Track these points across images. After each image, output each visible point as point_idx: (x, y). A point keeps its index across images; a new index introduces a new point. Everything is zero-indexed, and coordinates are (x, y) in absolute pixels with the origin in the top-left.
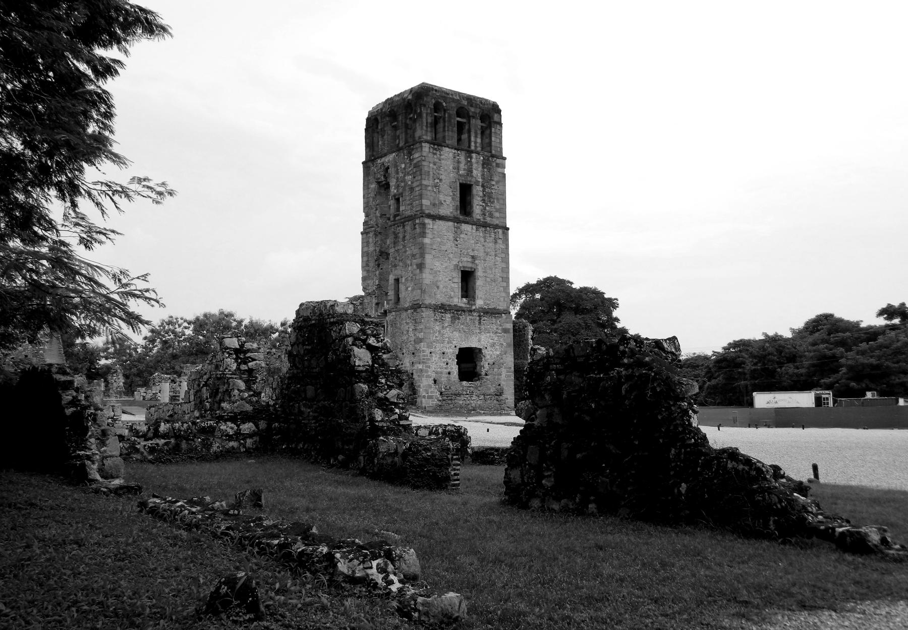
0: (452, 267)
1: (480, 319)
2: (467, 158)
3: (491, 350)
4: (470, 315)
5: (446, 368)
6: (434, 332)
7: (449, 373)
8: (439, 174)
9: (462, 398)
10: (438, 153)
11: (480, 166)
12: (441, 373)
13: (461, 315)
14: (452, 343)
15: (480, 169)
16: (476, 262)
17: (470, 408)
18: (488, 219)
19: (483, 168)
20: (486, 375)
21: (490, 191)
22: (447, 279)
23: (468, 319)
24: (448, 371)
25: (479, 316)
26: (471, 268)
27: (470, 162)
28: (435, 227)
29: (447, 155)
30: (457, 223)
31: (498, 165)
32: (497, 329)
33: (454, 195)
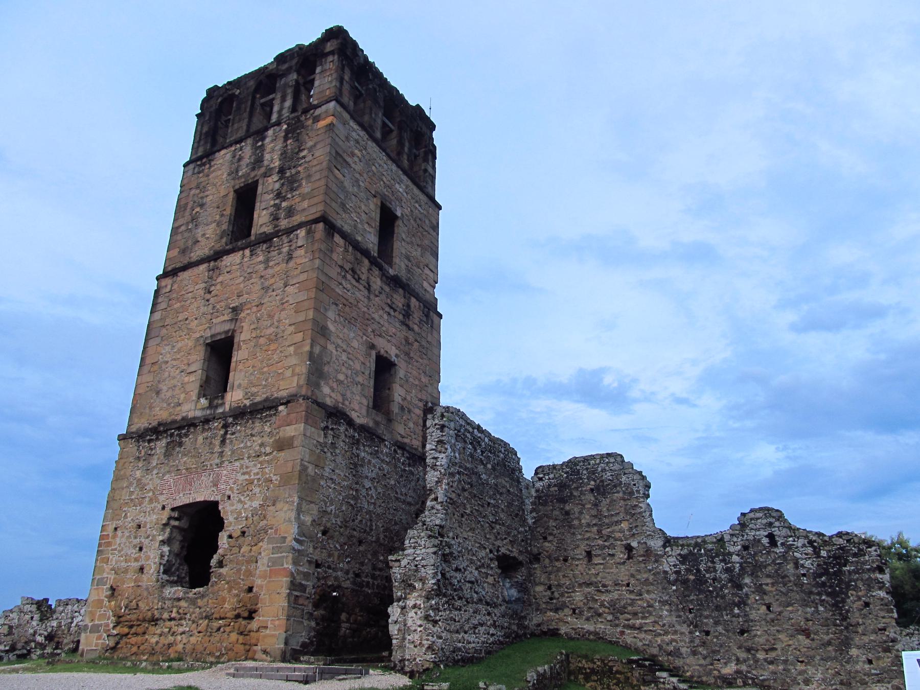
0: (191, 343)
1: (226, 433)
2: (257, 142)
3: (240, 501)
4: (204, 430)
5: (136, 560)
6: (131, 484)
7: (142, 569)
8: (202, 198)
9: (162, 628)
10: (208, 166)
11: (282, 139)
12: (126, 571)
13: (186, 435)
14: (157, 501)
15: (279, 145)
16: (242, 315)
17: (172, 656)
18: (284, 224)
19: (286, 138)
20: (221, 564)
21: (293, 171)
22: (178, 371)
23: (200, 438)
24: (140, 564)
25: (225, 426)
26: (229, 331)
27: (263, 145)
28: (175, 286)
29: (221, 161)
30: (215, 260)
31: (317, 119)
32: (262, 445)
33: (222, 215)
